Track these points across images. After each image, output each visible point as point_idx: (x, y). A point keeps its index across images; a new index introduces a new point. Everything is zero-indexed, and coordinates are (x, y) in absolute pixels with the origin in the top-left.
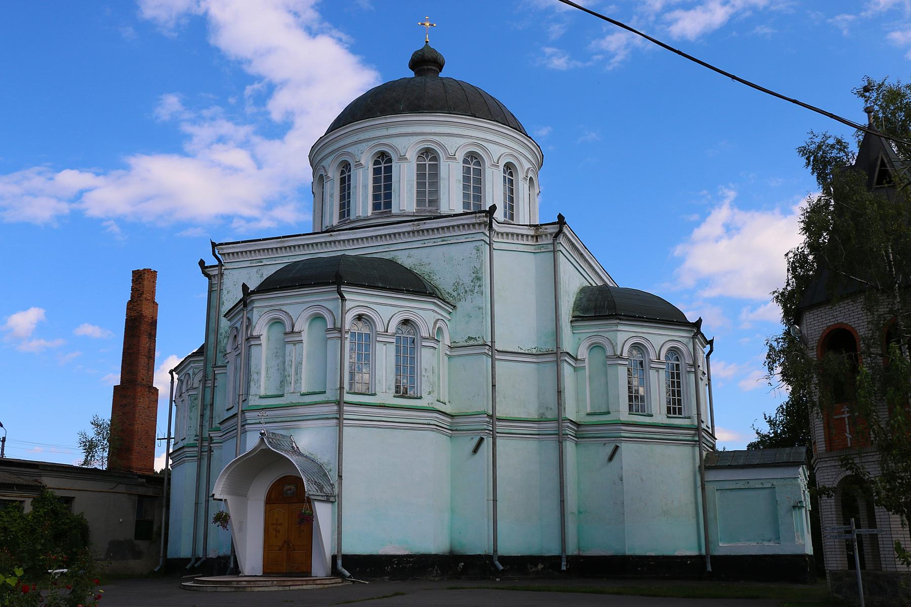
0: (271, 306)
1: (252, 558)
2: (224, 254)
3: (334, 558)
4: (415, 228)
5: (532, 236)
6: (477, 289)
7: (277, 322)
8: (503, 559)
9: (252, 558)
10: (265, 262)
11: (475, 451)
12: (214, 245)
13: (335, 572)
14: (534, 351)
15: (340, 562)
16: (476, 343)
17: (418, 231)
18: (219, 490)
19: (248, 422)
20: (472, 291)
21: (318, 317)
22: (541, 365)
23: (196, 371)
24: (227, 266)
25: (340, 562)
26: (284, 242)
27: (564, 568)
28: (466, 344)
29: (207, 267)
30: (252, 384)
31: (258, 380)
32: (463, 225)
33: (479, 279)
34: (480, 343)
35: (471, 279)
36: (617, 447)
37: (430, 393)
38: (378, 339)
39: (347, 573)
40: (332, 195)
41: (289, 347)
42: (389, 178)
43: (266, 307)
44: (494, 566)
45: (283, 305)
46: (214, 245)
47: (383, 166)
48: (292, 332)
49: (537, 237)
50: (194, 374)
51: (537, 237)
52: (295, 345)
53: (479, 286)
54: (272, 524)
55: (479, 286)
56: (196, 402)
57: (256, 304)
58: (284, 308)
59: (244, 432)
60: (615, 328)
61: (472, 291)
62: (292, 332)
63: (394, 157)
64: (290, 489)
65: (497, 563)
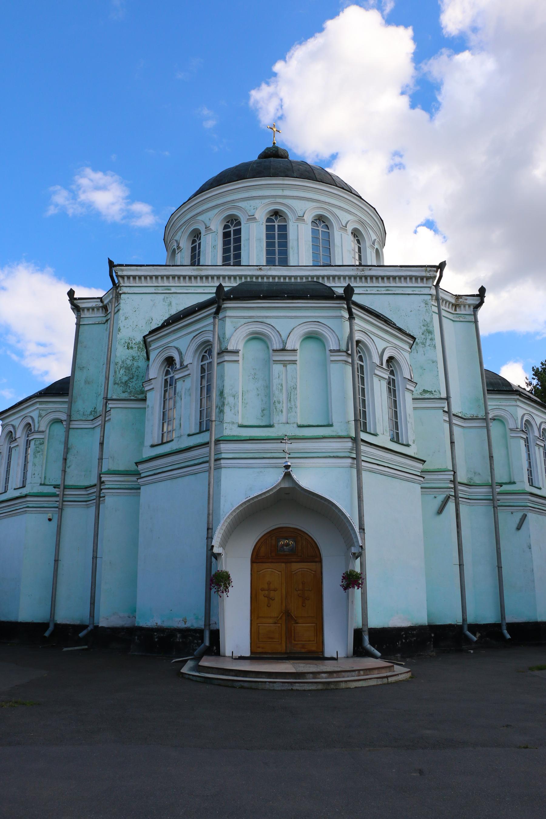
0: (250, 317)
1: (236, 634)
2: (123, 277)
3: (358, 633)
4: (360, 273)
5: (453, 305)
6: (428, 341)
7: (256, 337)
8: (474, 628)
9: (236, 634)
10: (173, 290)
11: (440, 511)
12: (111, 264)
13: (359, 651)
14: (460, 415)
15: (366, 638)
16: (431, 396)
17: (361, 278)
18: (216, 541)
19: (223, 456)
20: (423, 344)
21: (311, 337)
22: (467, 430)
23: (43, 413)
24: (125, 290)
25: (366, 638)
26: (201, 270)
27: (508, 636)
28: (421, 397)
29: (76, 299)
30: (226, 409)
31: (235, 405)
32: (411, 277)
33: (430, 332)
34: (437, 397)
35: (421, 331)
36: (525, 516)
37: (414, 442)
38: (377, 372)
39: (379, 654)
40: (214, 247)
41: (277, 369)
42: (284, 236)
43: (244, 317)
44: (466, 637)
45: (267, 317)
46: (111, 264)
47: (276, 224)
48: (284, 350)
49: (456, 306)
50: (40, 416)
51: (456, 306)
52: (285, 366)
53: (431, 339)
54: (263, 590)
55: (431, 339)
56: (41, 447)
57: (229, 313)
58: (268, 321)
59: (218, 468)
60: (514, 403)
61: (423, 344)
62: (284, 350)
63: (290, 215)
64: (287, 545)
65: (468, 633)
